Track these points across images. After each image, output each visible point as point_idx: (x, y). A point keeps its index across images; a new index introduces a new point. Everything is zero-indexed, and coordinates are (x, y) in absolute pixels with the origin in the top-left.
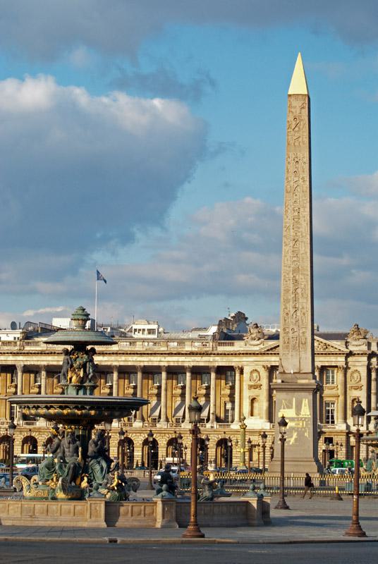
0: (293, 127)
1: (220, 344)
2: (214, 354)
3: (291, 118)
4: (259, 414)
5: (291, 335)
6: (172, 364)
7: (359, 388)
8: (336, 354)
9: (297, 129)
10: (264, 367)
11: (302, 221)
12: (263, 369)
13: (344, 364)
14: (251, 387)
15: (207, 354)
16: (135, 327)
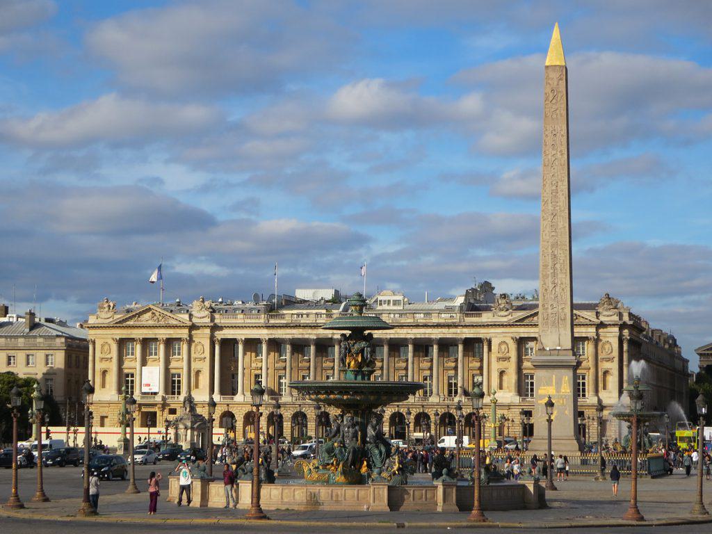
0: (551, 99)
1: (467, 315)
2: (462, 326)
3: (549, 90)
4: (508, 387)
5: (550, 311)
6: (419, 336)
7: (610, 360)
8: (586, 325)
9: (554, 101)
10: (512, 338)
11: (560, 193)
12: (512, 341)
13: (594, 335)
14: (499, 359)
15: (455, 326)
16: (380, 298)
